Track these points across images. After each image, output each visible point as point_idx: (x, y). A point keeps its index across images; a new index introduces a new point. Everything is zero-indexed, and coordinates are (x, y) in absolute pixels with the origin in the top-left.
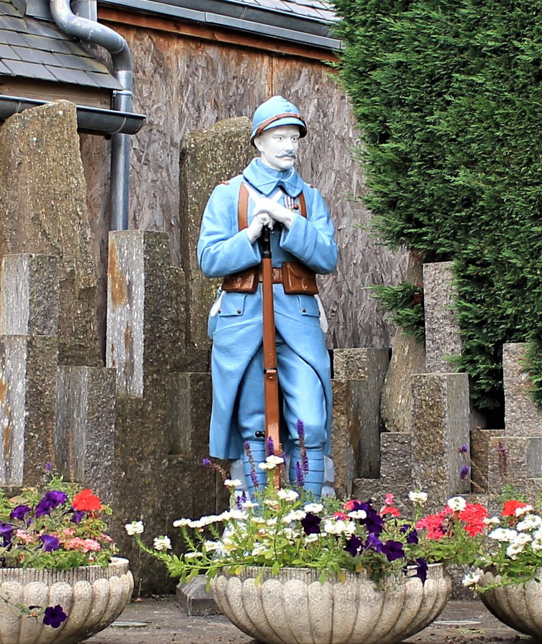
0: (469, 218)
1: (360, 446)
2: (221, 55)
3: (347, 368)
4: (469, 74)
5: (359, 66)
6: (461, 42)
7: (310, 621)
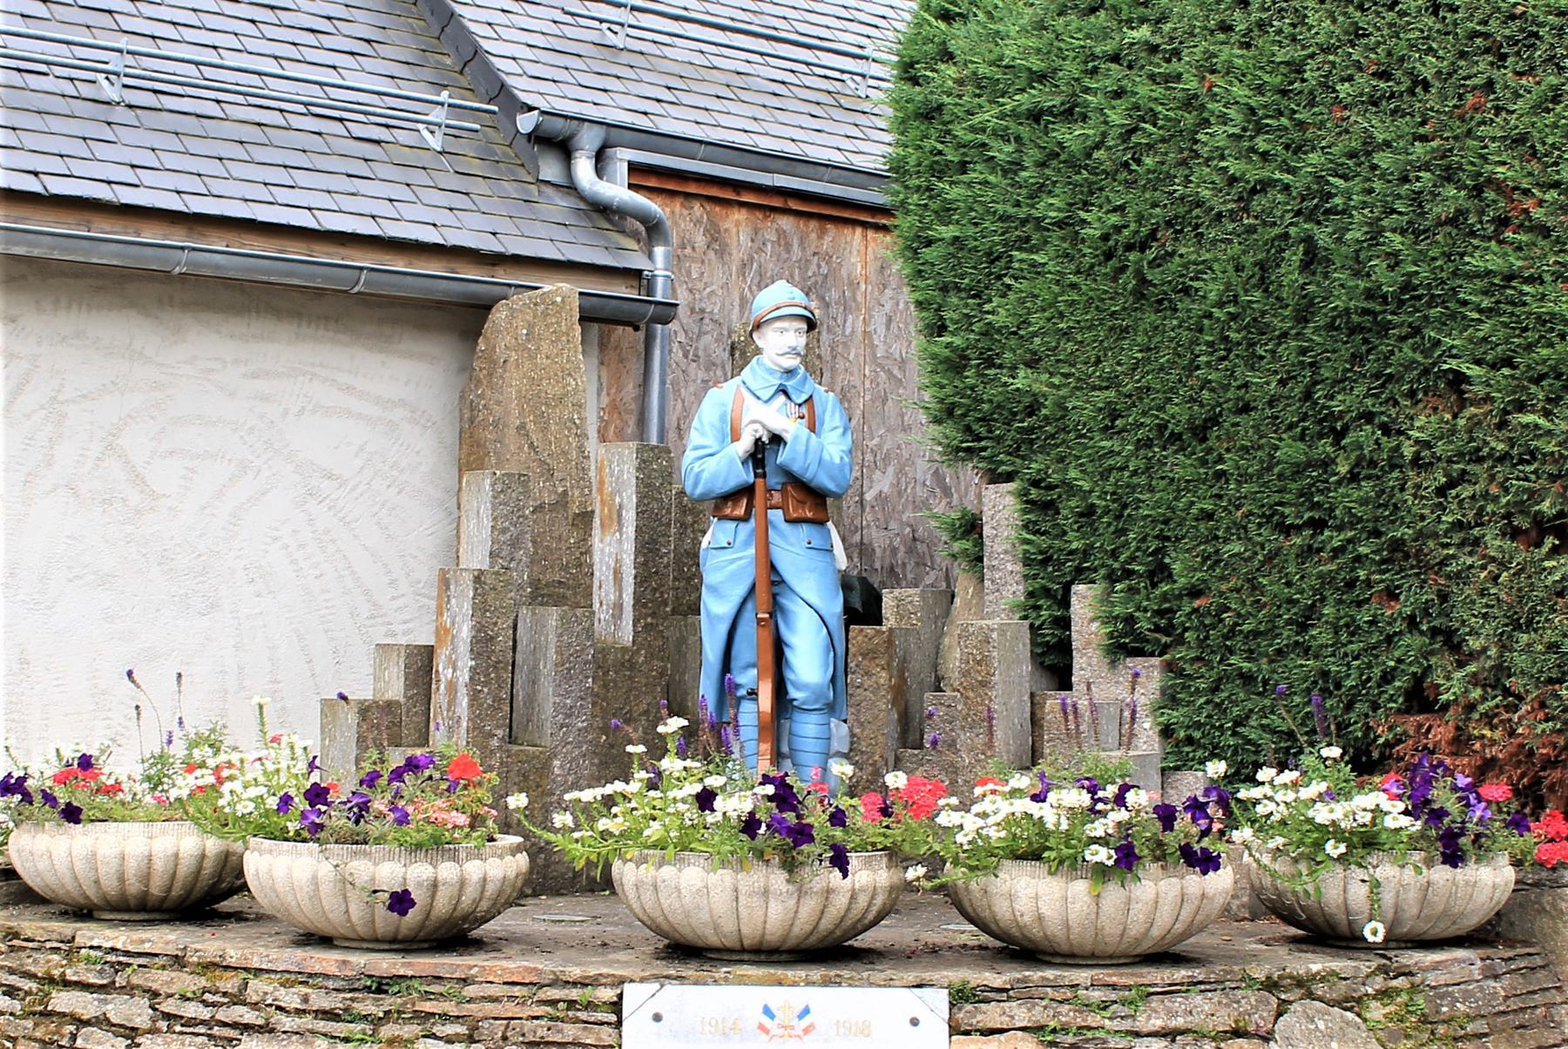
0: (1031, 430)
1: (906, 708)
2: (798, 227)
3: (898, 613)
4: (1032, 252)
5: (913, 242)
6: (1022, 213)
7: (711, 916)
